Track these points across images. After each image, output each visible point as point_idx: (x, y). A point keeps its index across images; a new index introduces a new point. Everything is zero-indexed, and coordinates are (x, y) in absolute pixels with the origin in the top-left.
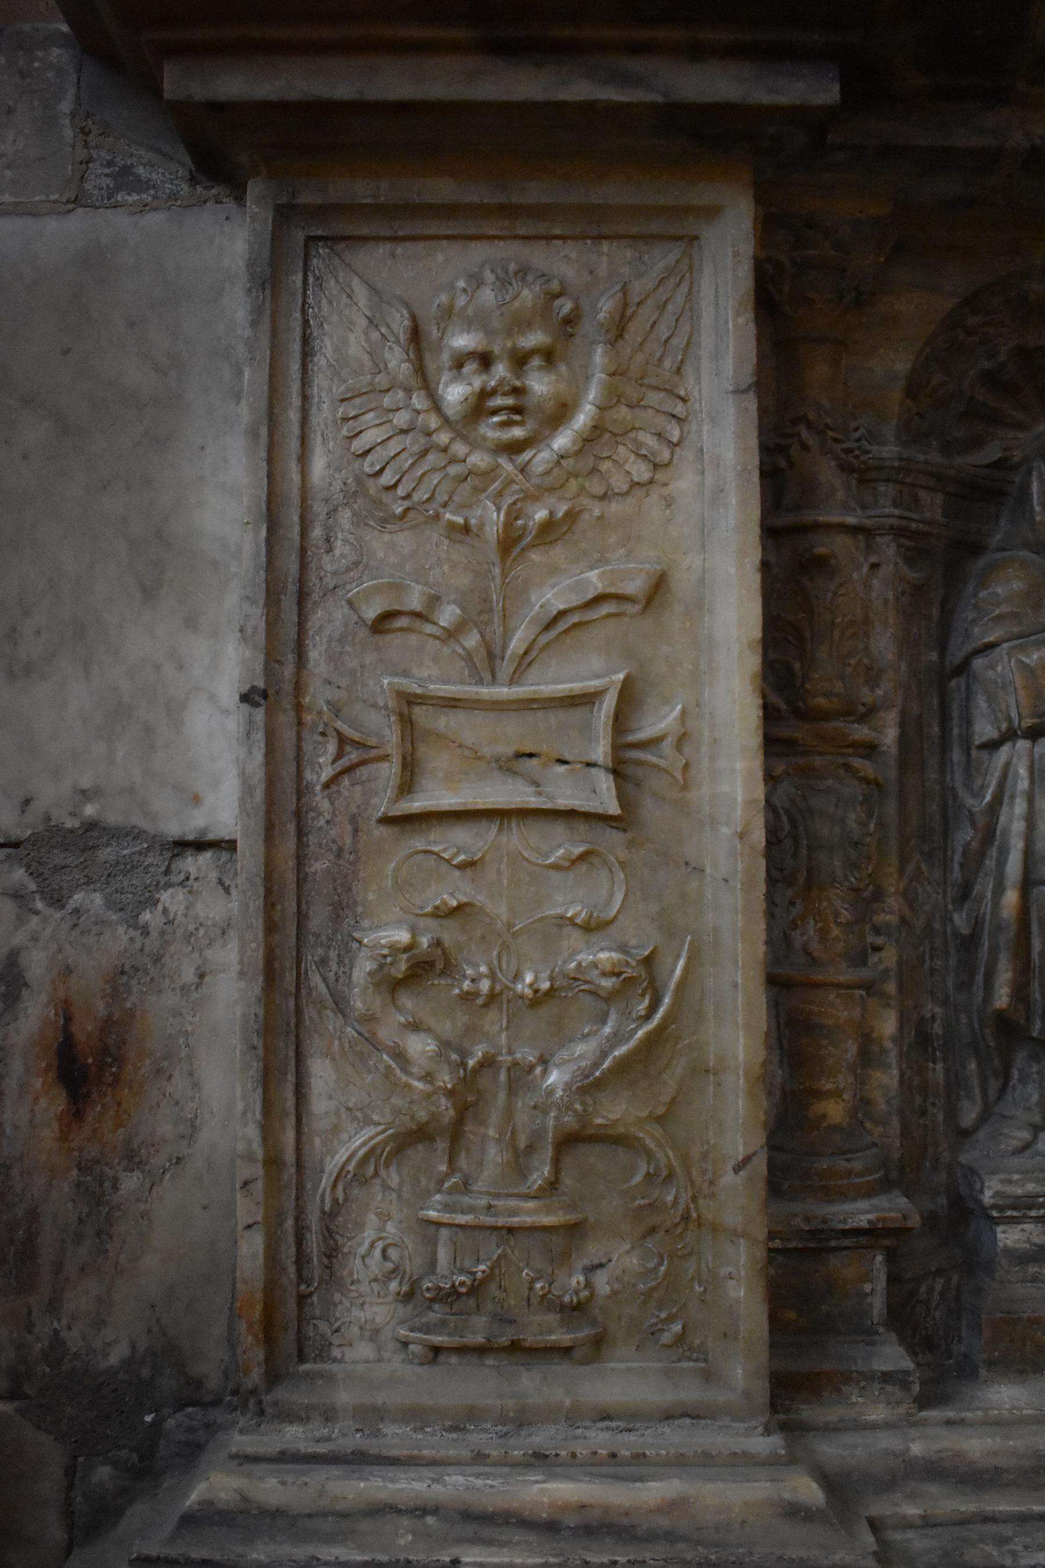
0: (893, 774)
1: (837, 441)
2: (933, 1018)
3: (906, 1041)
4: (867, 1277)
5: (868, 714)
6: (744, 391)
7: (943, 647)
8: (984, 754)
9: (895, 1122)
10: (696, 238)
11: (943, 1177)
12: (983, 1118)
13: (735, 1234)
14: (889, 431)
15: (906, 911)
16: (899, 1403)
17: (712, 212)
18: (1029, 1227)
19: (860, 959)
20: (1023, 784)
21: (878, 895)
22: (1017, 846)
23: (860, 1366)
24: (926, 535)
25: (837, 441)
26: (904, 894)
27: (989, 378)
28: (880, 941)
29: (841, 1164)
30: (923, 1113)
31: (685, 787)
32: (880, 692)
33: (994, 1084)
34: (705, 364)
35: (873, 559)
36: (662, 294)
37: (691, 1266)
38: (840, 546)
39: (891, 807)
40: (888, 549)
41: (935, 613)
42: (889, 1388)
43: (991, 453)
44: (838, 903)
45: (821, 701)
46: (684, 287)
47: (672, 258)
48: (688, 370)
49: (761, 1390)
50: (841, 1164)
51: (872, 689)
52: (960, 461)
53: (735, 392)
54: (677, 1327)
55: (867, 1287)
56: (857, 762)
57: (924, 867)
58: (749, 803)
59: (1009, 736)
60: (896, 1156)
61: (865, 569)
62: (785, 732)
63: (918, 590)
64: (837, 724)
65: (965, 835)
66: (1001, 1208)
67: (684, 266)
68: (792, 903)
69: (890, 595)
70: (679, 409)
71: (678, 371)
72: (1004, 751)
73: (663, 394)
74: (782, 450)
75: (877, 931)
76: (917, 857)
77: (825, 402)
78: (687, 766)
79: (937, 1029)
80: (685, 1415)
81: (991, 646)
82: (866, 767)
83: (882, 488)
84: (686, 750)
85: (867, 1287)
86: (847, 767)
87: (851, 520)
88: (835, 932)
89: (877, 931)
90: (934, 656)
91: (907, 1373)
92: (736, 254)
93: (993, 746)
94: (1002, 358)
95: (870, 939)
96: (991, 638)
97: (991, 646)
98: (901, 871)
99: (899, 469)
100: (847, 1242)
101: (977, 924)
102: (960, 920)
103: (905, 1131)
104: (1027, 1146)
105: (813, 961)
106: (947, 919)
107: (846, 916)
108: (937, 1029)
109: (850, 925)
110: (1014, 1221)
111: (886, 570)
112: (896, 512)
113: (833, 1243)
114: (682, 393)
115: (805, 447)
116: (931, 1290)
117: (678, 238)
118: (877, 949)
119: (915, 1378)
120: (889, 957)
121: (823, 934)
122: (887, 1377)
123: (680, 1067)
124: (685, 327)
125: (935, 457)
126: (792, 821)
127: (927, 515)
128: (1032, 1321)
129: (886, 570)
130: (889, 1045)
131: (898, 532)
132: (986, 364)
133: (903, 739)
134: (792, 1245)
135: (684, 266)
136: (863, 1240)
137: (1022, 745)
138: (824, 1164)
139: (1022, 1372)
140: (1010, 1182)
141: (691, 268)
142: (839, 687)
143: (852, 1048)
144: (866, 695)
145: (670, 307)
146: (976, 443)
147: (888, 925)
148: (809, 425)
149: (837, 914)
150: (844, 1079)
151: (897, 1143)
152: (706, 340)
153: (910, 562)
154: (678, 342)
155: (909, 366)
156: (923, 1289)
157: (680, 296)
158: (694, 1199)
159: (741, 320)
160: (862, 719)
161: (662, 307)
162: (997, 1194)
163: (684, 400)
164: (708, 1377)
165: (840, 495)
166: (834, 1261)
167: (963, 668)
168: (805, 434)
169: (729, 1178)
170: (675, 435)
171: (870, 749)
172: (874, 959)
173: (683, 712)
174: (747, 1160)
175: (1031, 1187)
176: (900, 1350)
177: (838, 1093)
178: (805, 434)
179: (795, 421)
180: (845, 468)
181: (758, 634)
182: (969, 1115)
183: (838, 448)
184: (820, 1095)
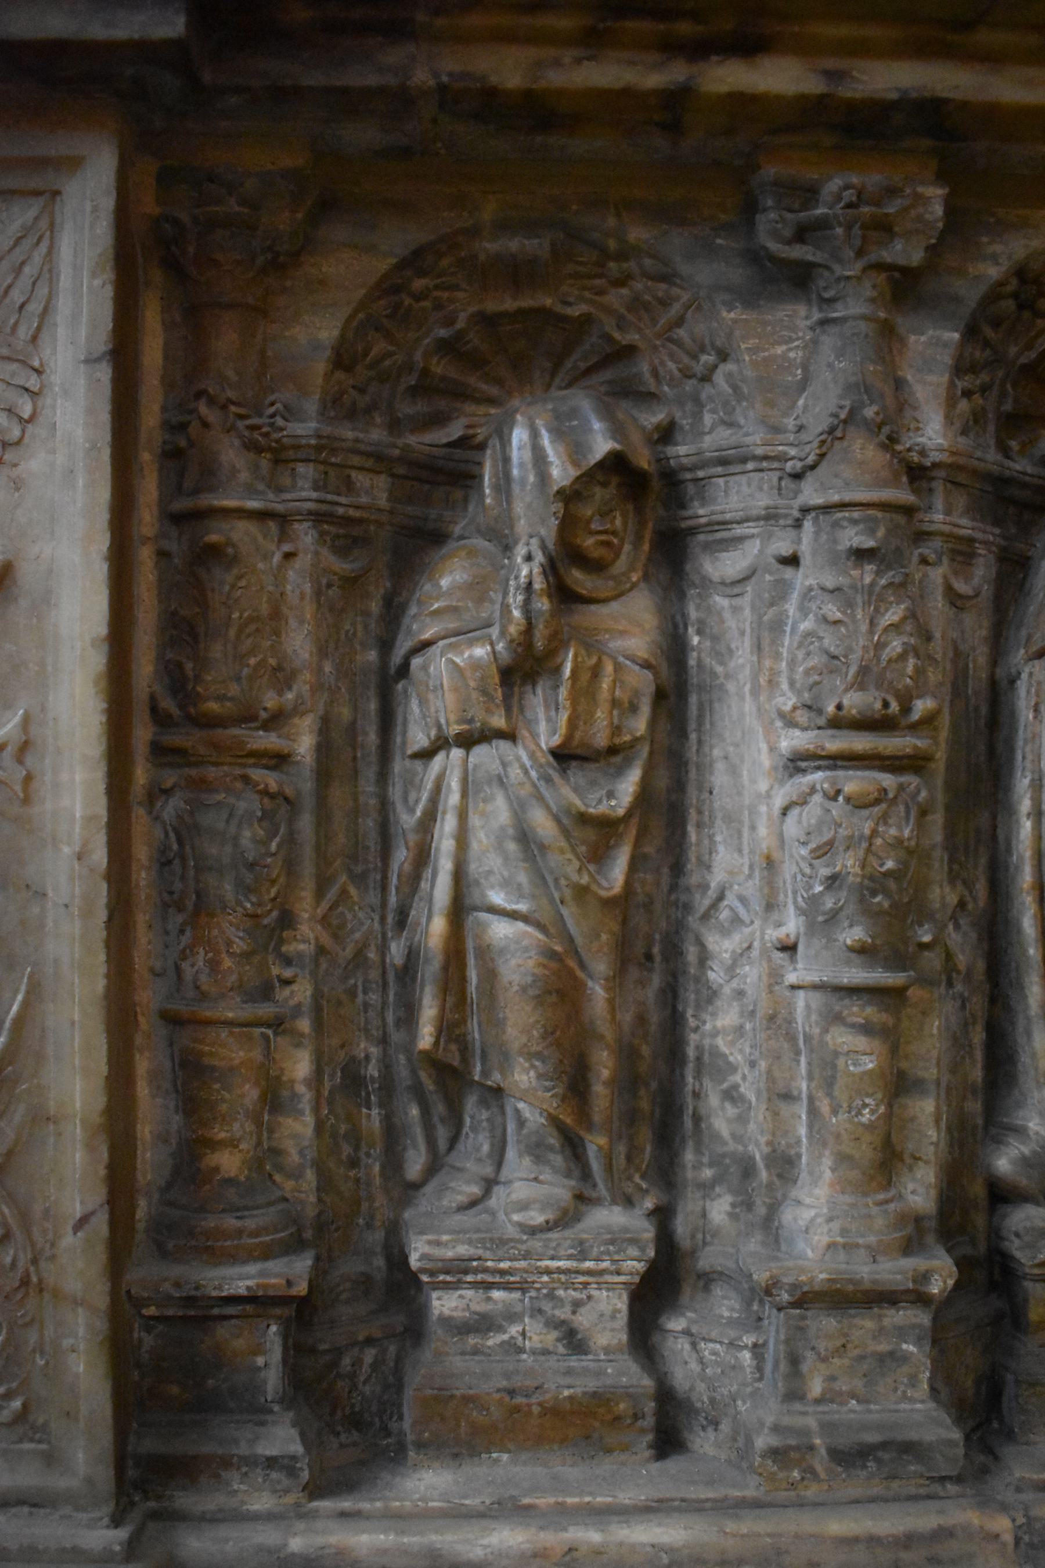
0: (307, 785)
1: (242, 417)
2: (367, 1058)
3: (327, 1085)
4: (258, 1350)
5: (276, 720)
6: (98, 360)
7: (386, 646)
8: (418, 765)
9: (310, 1175)
10: (57, 193)
11: (379, 1235)
12: (433, 1168)
13: (76, 1303)
14: (311, 406)
15: (326, 940)
16: (286, 1491)
17: (73, 164)
18: (469, 1293)
19: (265, 992)
20: (454, 798)
21: (287, 920)
22: (445, 866)
23: (243, 1450)
24: (360, 521)
25: (242, 417)
26: (324, 921)
27: (447, 347)
28: (288, 973)
29: (231, 1222)
30: (354, 1163)
31: (26, 801)
32: (290, 696)
33: (442, 1134)
34: (61, 332)
35: (287, 548)
36: (18, 255)
37: (33, 1337)
38: (242, 532)
39: (306, 823)
40: (306, 536)
41: (375, 607)
42: (274, 1475)
43: (455, 431)
44: (231, 932)
45: (213, 706)
46: (43, 248)
47: (32, 213)
48: (45, 336)
49: (105, 1476)
50: (231, 1222)
51: (280, 693)
52: (412, 440)
53: (87, 361)
54: (17, 1404)
55: (260, 1361)
56: (257, 774)
57: (353, 891)
58: (89, 819)
59: (440, 744)
60: (311, 1212)
61: (277, 558)
62: (175, 739)
63: (351, 583)
64: (235, 731)
65: (401, 856)
66: (432, 1273)
67: (43, 224)
68: (182, 932)
69: (308, 588)
70: (33, 383)
71: (34, 338)
72: (439, 759)
73: (15, 366)
74: (182, 427)
75: (288, 961)
76: (344, 878)
77: (230, 374)
78: (28, 779)
79: (373, 1070)
80: (21, 1502)
81: (427, 644)
82: (271, 780)
83: (301, 468)
84: (29, 760)
85: (260, 1361)
86: (246, 779)
87: (253, 504)
88: (227, 963)
89: (288, 961)
90: (373, 656)
91: (294, 1458)
92: (95, 209)
93: (426, 755)
94: (460, 324)
95: (275, 971)
96: (426, 636)
97: (427, 644)
98: (320, 894)
99: (319, 448)
100: (230, 1310)
101: (412, 956)
102: (397, 951)
103: (325, 1184)
104: (473, 1204)
105: (203, 996)
106: (383, 949)
107: (240, 945)
108: (373, 1070)
109: (247, 955)
110: (446, 1286)
111: (304, 561)
112: (314, 495)
113: (216, 1311)
114: (36, 364)
115: (206, 425)
116: (357, 1363)
117: (37, 193)
118: (287, 982)
119: (303, 1464)
120: (302, 992)
121: (214, 965)
122: (271, 1462)
123: (19, 1113)
124: (43, 291)
125: (377, 435)
126: (180, 842)
127: (364, 500)
128: (467, 1399)
129: (304, 561)
130: (301, 1089)
131: (318, 518)
132: (443, 333)
133: (324, 748)
134: (170, 1312)
135: (43, 224)
136: (249, 1308)
137: (457, 753)
138: (211, 1222)
139: (456, 1456)
140: (438, 1243)
141: (52, 226)
142: (234, 689)
143: (250, 1094)
144: (270, 701)
145: (27, 269)
146: (439, 420)
147: (300, 955)
148: (212, 401)
149: (229, 943)
150: (241, 1127)
151: (313, 1199)
152: (64, 306)
153: (342, 551)
154: (35, 307)
155: (336, 333)
156: (346, 1361)
157: (37, 257)
158: (35, 1261)
159: (97, 282)
160: (266, 726)
161: (18, 270)
162: (423, 1257)
163: (39, 372)
164: (50, 1459)
165: (244, 476)
166: (222, 1331)
167: (404, 671)
168: (203, 409)
169: (69, 1240)
170: (26, 412)
171: (280, 760)
172: (282, 994)
173: (26, 721)
174: (82, 1222)
175: (463, 1250)
176: (294, 1432)
177: (232, 1144)
178: (203, 409)
179: (199, 394)
180: (252, 447)
181: (103, 630)
182: (415, 1164)
183: (241, 424)
184: (213, 1145)
